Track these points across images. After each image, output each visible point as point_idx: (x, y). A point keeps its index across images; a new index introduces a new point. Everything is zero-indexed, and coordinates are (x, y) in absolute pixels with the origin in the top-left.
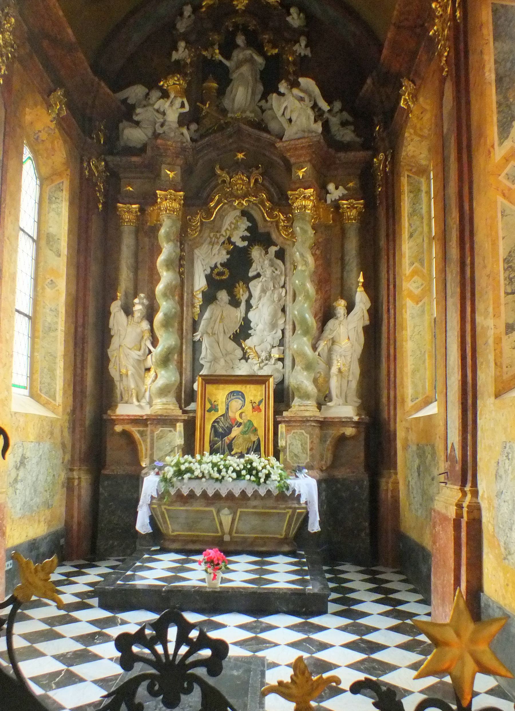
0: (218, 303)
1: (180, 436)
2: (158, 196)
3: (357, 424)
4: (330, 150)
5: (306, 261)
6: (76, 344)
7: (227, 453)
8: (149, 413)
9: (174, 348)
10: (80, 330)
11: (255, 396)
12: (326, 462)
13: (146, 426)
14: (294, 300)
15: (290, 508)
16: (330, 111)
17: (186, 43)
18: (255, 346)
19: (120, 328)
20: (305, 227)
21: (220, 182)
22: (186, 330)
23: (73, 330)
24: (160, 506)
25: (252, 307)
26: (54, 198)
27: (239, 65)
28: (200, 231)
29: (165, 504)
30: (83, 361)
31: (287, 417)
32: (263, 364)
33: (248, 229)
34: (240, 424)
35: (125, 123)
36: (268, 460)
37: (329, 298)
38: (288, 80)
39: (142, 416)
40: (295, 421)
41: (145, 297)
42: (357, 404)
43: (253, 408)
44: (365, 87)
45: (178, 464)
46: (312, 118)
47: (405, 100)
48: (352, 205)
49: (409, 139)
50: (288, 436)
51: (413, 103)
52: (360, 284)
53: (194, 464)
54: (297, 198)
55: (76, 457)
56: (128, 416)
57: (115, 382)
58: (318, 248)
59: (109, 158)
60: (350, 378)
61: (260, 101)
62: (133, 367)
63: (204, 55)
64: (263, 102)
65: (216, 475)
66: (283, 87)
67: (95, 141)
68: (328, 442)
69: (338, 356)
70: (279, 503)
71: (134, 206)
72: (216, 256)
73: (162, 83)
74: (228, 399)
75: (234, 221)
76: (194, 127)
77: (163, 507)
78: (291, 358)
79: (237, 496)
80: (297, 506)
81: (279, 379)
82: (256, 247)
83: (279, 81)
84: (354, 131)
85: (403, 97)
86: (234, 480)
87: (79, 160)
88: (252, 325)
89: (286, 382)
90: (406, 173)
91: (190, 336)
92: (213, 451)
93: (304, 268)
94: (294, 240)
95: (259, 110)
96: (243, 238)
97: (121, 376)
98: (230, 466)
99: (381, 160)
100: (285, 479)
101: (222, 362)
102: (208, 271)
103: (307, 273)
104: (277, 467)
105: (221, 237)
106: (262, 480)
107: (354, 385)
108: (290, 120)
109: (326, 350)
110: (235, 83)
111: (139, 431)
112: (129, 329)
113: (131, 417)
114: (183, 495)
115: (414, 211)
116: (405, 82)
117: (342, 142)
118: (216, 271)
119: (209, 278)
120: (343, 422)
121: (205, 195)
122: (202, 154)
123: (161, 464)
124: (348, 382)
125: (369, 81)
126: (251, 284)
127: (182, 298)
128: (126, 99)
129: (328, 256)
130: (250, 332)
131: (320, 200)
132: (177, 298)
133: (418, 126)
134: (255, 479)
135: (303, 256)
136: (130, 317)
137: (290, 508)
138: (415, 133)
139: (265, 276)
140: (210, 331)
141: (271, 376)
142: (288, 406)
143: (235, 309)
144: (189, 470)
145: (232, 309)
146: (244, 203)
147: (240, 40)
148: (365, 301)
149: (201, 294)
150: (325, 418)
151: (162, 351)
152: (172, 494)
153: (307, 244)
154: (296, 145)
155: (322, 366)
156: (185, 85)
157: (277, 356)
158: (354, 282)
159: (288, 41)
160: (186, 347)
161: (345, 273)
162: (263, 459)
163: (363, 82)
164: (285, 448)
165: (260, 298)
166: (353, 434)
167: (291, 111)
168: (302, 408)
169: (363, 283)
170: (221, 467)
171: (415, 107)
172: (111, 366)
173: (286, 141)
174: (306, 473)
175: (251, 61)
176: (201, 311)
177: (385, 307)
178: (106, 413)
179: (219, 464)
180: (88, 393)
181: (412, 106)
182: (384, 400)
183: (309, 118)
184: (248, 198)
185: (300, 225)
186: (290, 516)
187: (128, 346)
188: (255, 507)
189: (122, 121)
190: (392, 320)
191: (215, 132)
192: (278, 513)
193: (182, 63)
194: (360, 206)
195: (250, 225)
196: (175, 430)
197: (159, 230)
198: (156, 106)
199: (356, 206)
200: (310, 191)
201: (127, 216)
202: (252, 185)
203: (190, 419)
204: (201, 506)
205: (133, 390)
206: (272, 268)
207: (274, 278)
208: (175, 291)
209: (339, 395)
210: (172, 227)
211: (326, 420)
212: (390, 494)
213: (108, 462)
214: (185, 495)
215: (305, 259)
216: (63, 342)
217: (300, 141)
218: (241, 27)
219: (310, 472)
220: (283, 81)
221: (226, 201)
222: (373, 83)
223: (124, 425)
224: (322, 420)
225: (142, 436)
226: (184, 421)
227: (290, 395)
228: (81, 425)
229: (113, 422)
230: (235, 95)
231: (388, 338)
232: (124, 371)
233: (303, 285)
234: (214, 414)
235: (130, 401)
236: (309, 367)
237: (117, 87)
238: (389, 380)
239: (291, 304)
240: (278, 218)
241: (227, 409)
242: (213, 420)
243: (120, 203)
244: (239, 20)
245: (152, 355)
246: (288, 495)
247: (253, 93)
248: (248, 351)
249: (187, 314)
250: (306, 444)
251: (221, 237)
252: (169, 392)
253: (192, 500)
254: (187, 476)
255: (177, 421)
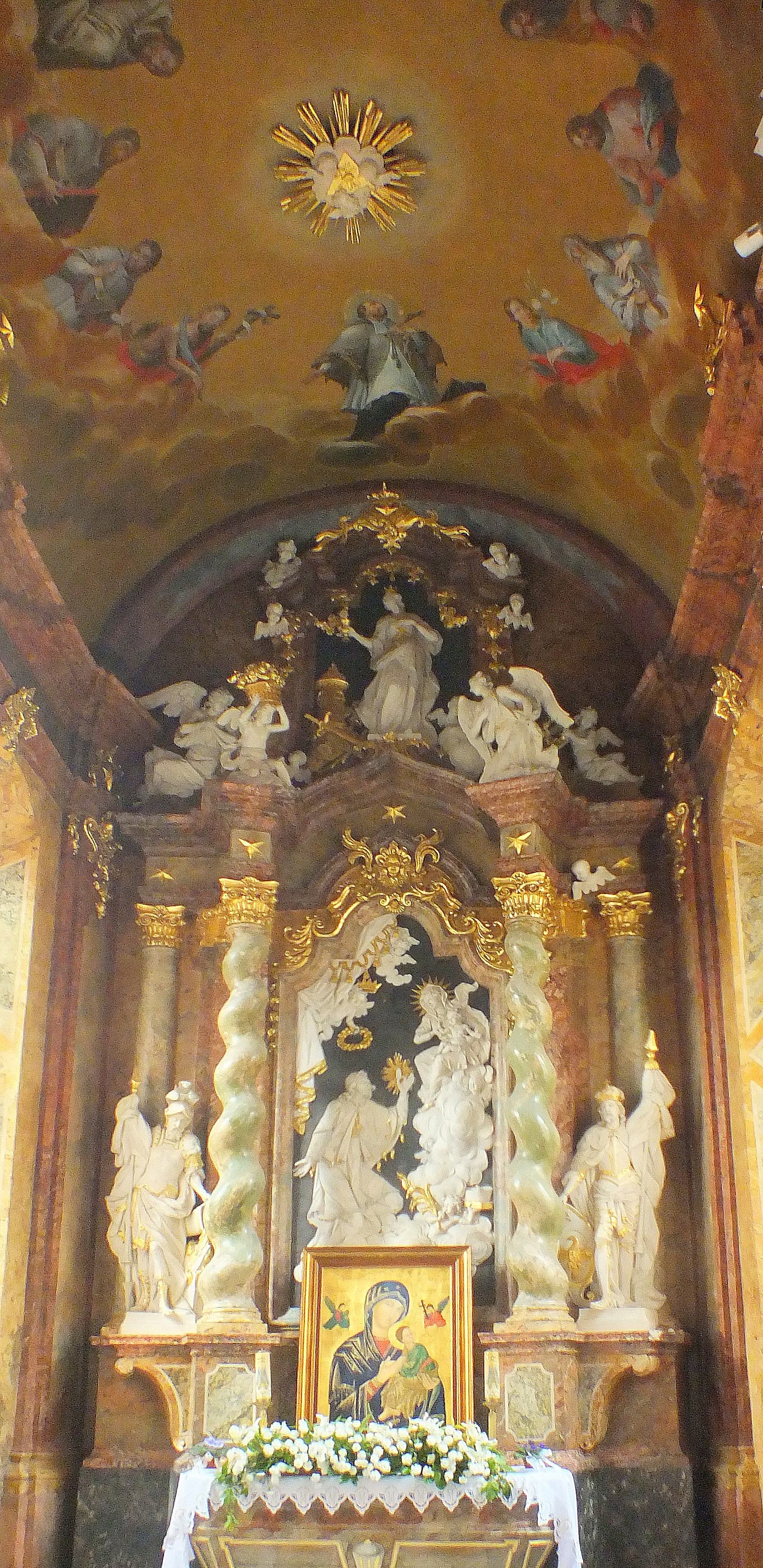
0: (349, 1097)
1: (263, 1381)
2: (224, 889)
3: (660, 1347)
4: (577, 799)
5: (532, 1011)
6: (37, 1187)
7: (369, 1415)
8: (193, 1331)
9: (252, 1192)
10: (47, 1156)
11: (431, 1291)
12: (593, 1432)
13: (189, 1360)
14: (512, 1090)
15: (515, 1537)
16: (574, 727)
17: (284, 607)
18: (429, 1185)
19: (135, 1152)
20: (529, 945)
21: (352, 862)
22: (279, 1154)
23: (31, 1157)
24: (215, 1538)
25: (421, 1104)
26: (4, 893)
27: (391, 645)
28: (312, 956)
29: (227, 1534)
30: (50, 1221)
31: (503, 1336)
32: (448, 1223)
33: (412, 952)
34: (399, 1353)
35: (159, 752)
36: (463, 1431)
37: (586, 1085)
38: (487, 673)
39: (179, 1339)
40: (519, 1344)
41: (190, 1088)
42: (657, 1305)
43: (427, 1317)
44: (644, 683)
45: (257, 1444)
46: (539, 742)
47: (723, 704)
48: (626, 901)
49: (736, 775)
50: (507, 1376)
51: (740, 708)
52: (651, 1056)
53: (293, 1441)
54: (511, 891)
55: (28, 1430)
56: (148, 1338)
57: (121, 1265)
58: (559, 986)
59: (123, 817)
60: (640, 1249)
61: (432, 710)
62: (162, 1232)
63: (320, 629)
64: (440, 712)
65: (343, 1466)
66: (478, 684)
67: (95, 785)
68: (596, 1389)
69: (611, 1203)
70: (489, 1526)
71: (172, 909)
72: (345, 1004)
73: (234, 679)
74: (370, 1299)
75: (383, 936)
76: (299, 758)
77: (222, 1540)
78: (509, 1209)
79: (392, 1512)
80: (530, 1532)
81: (483, 1256)
82: (430, 986)
83: (470, 674)
84: (624, 764)
85: (718, 698)
86: (384, 1475)
87: (60, 819)
88: (422, 1141)
89: (500, 1261)
90: (734, 839)
91: (287, 1166)
92: (337, 1413)
93: (530, 1025)
94: (508, 971)
95: (432, 727)
96: (402, 969)
97: (134, 1252)
98: (376, 1445)
99: (681, 816)
100: (502, 1471)
101: (358, 1218)
102: (329, 1035)
103: (536, 1036)
104: (483, 1446)
105: (356, 967)
106: (449, 1476)
107: (648, 1263)
108: (495, 746)
109: (584, 1191)
110: (380, 681)
111: (170, 1372)
112: (155, 1154)
113: (152, 1342)
114: (269, 1512)
115: (755, 910)
116: (722, 672)
117: (599, 784)
118: (344, 1034)
119: (329, 1047)
120: (628, 1343)
121: (322, 885)
122: (314, 809)
123: (219, 1444)
124: (635, 1256)
125: (650, 672)
126: (420, 1060)
127: (271, 1090)
128: (160, 709)
129: (581, 1004)
130: (417, 1156)
131: (560, 893)
132: (260, 1088)
133: (753, 750)
134: (432, 1474)
135: (529, 1002)
136: (158, 1129)
137: (515, 1537)
138: (748, 764)
139: (448, 1043)
140: (330, 1155)
141: (466, 1248)
142: (505, 1312)
143: (386, 1109)
144: (284, 1457)
145: (379, 1109)
146: (403, 900)
147: (392, 602)
148: (661, 1088)
149: (312, 1081)
150: (587, 1336)
151: (225, 1197)
152: (244, 1509)
153: (537, 978)
154: (507, 790)
155: (576, 1224)
156: (280, 682)
157: (478, 1206)
158: (638, 1052)
159: (487, 603)
160: (279, 1188)
161: (618, 1033)
162: (450, 1429)
163: (642, 671)
164: (501, 1402)
165: (439, 1087)
166: (652, 1368)
167: (497, 728)
168: (537, 1315)
169: (656, 1053)
170: (356, 1448)
171: (745, 716)
172: (112, 1233)
173: (488, 783)
174: (549, 1458)
175: (414, 638)
176: (311, 1116)
177: (705, 1100)
178: (98, 1333)
179: (350, 1440)
180: (59, 1289)
181: (737, 714)
182: (716, 1294)
183: (532, 740)
184: (411, 891)
185: (520, 942)
186: (514, 1555)
187: (153, 1190)
188: (432, 1537)
189: (151, 749)
190: (722, 1128)
191: (341, 768)
192: (488, 1550)
193: (275, 642)
194: (642, 903)
195: (416, 942)
196: (252, 1367)
197: (225, 953)
198: (222, 721)
199: (633, 903)
200: (539, 876)
201: (156, 928)
202: (418, 867)
203: (285, 1344)
204: (310, 1537)
205: (160, 1283)
206: (464, 1026)
207: (467, 1047)
208: (256, 1075)
209: (616, 1286)
210: (251, 947)
211: (591, 1340)
212: (739, 1499)
213: (98, 1441)
214: (274, 1511)
215: (532, 1007)
216: (9, 1182)
217: (514, 784)
218: (392, 579)
219: (558, 1455)
220: (479, 673)
221: (365, 898)
222: (659, 676)
223: (138, 1360)
224: (582, 1340)
225: (176, 1383)
226: (273, 1348)
227: (510, 1289)
228: (40, 1360)
229: (113, 1352)
230: (383, 702)
231: (717, 1164)
232: (140, 1242)
233: (530, 1058)
234: (340, 1333)
235: (152, 1305)
236: (547, 1226)
237: (141, 688)
238: (723, 1252)
239: (505, 1098)
240: (474, 928)
241: (370, 1320)
242: (338, 1345)
243: (141, 903)
244: (391, 567)
245: (203, 1208)
246: (510, 1508)
247: (419, 698)
248: (415, 1195)
249: (282, 1122)
250: (546, 1393)
251: (356, 967)
252: (241, 1285)
253: (289, 1524)
254: (277, 1469)
255: (257, 1347)
